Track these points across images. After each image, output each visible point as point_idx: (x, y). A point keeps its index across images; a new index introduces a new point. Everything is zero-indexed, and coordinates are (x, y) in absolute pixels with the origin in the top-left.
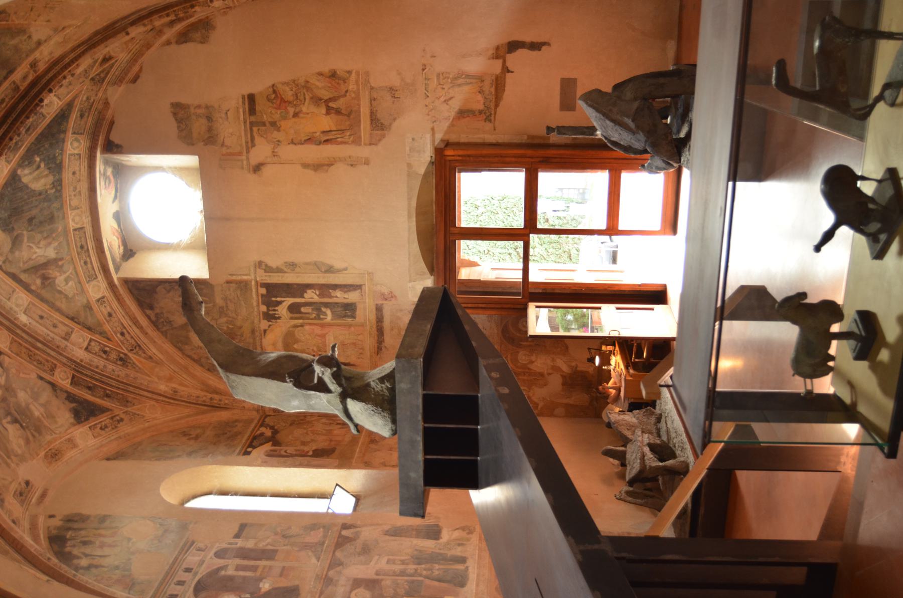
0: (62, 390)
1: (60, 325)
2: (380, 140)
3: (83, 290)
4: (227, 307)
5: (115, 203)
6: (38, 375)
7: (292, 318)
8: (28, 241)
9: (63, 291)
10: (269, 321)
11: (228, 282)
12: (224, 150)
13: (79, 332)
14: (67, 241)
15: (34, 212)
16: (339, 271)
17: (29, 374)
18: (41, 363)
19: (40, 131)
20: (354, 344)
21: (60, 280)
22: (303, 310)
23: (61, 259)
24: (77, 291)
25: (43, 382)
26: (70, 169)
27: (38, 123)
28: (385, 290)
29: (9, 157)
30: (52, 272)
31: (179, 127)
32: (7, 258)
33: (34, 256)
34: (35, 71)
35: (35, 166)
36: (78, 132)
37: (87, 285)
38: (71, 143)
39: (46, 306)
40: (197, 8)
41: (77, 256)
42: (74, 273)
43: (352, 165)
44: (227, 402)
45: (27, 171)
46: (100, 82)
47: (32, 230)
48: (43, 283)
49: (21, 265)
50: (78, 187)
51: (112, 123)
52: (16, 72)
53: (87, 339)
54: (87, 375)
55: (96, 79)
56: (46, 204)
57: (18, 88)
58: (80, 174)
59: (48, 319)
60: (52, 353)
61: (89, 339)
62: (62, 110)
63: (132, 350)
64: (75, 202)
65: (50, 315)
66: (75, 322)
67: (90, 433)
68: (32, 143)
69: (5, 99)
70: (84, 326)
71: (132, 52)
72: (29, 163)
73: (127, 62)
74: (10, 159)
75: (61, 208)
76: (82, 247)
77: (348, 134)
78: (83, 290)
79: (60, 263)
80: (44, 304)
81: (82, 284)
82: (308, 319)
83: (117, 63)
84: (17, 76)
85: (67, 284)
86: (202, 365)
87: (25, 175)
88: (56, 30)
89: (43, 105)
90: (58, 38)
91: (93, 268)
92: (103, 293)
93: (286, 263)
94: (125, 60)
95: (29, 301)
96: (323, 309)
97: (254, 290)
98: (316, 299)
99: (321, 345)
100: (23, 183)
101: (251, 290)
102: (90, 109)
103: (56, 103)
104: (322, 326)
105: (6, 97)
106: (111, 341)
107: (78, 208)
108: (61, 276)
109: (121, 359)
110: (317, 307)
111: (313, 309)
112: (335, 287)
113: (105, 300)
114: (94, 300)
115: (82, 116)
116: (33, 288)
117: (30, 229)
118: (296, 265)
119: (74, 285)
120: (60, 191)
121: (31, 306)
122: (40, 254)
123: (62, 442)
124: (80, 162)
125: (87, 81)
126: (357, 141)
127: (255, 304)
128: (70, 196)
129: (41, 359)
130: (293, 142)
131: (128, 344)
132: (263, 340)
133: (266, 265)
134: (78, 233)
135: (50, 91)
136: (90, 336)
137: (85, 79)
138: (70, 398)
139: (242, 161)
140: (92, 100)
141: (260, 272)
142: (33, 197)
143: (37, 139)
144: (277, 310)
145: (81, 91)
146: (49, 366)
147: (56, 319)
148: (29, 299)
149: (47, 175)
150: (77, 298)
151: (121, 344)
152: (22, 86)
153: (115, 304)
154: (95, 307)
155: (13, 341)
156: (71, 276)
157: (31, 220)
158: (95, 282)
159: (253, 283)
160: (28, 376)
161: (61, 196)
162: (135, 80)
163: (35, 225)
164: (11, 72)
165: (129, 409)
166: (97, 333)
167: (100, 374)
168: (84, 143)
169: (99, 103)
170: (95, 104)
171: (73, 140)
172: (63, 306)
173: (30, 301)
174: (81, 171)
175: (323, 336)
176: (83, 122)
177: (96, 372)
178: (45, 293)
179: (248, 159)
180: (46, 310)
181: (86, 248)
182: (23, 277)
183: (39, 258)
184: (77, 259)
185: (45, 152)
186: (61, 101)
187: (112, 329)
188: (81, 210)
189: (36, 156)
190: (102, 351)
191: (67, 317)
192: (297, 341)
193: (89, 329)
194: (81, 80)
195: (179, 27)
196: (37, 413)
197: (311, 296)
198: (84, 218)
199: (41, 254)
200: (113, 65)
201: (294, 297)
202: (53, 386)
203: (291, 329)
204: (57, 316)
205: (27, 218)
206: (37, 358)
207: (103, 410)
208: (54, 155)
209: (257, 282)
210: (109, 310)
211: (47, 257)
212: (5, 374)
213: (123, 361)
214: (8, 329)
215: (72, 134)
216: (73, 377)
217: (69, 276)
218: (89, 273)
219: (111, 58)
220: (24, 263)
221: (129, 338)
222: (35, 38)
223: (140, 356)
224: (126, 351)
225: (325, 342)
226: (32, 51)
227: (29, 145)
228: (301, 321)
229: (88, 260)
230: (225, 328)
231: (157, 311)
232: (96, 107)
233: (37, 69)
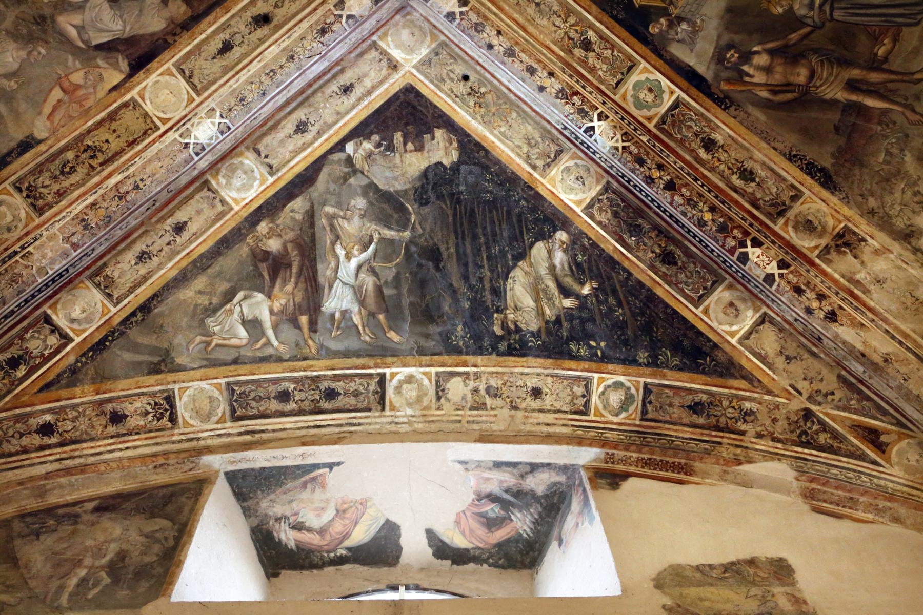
1: (143, 271)
3: (214, 364)
5: (425, 541)
6: (40, 142)
8: (382, 240)
9: (228, 306)
13: (103, 315)
17: (50, 116)
18: (62, 173)
19: (659, 292)
23: (313, 326)
24: (217, 345)
25: (13, 144)
26: (549, 380)
27: (680, 286)
29: (600, 209)
32: (355, 171)
33: (340, 252)
35: (569, 281)
36: (650, 402)
37: (223, 381)
38: (618, 385)
39: (202, 249)
41: (309, 373)
42: (269, 351)
45: (559, 257)
46: (800, 436)
47: (408, 255)
48: (267, 253)
49: (329, 209)
50: (498, 402)
51: (681, 482)
52: (825, 194)
53: (72, 330)
55: (809, 425)
56: (467, 305)
57: (781, 214)
58: (533, 410)
59: (169, 244)
61: (71, 334)
62: (716, 346)
64: (457, 388)
65: (179, 253)
66: (133, 314)
68: (630, 274)
69: (753, 180)
70: (113, 332)
71: (915, 492)
73: (877, 485)
74: (595, 211)
76: (331, 394)
78: (214, 366)
79: (304, 320)
80: (211, 243)
81: (232, 367)
83: (871, 466)
85: (244, 323)
87: (550, 252)
89: (746, 247)
91: (263, 416)
92: (187, 425)
94: (882, 483)
95: (233, 205)
100: (532, 245)
102: (718, 428)
103: (735, 328)
105: (759, 184)
106: (40, 390)
107: (439, 398)
108: (272, 312)
113: (165, 421)
114: (176, 387)
115: (696, 408)
116: (263, 227)
117: (413, 249)
119: (234, 342)
120: (494, 349)
121: (220, 208)
122: (341, 267)
124: (566, 412)
125: (799, 403)
128: (477, 376)
129: (74, 178)
131: (11, 432)
134: (372, 388)
136: (78, 340)
137: (805, 395)
140: (743, 427)
142: (492, 271)
143: (641, 284)
145: (769, 392)
146: (45, 191)
147: (160, 266)
148: (237, 208)
149: (543, 314)
150: (199, 339)
151: (18, 411)
152: (786, 223)
154: (154, 384)
156: (263, 340)
158: (223, 407)
160: (47, 109)
161: (480, 351)
162: (818, 510)
163: (420, 266)
164: (827, 181)
166: (77, 361)
168: (620, 424)
169: (737, 446)
170: (733, 436)
171: (629, 389)
172: (187, 294)
173: (232, 209)
174: (541, 415)
176: (676, 413)
178: (243, 250)
180: (192, 247)
181: (325, 405)
182: (298, 205)
183: (333, 264)
184: (302, 374)
185: (604, 308)
186: (740, 342)
187: (74, 407)
188: (434, 406)
189: (595, 285)
190: (20, 357)
191: (155, 296)
193: (99, 347)
194: (803, 386)
198: (409, 412)
200: (862, 457)
204: (168, 270)
205: (443, 248)
206: (81, 171)
208: (592, 337)
210: (133, 422)
211: (331, 287)
212: (81, 45)
215: (646, 385)
217: (263, 333)
218: (254, 399)
219: (881, 448)
220: (332, 218)
221: (25, 441)
226: (885, 224)
227: (626, 264)
229: (292, 406)
231: (86, 517)
232: (725, 441)
233: (833, 255)
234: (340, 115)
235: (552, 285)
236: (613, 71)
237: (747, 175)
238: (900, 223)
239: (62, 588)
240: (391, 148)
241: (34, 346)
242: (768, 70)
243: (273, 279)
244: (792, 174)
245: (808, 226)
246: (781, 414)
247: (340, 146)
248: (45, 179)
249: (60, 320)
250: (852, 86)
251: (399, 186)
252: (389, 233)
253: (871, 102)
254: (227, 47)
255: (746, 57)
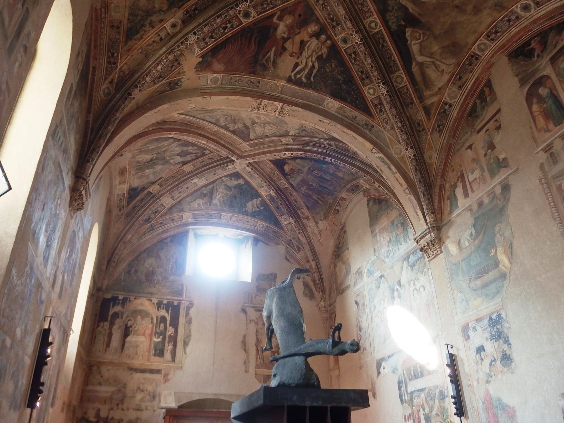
0: (149, 186)
1: (180, 195)
2: (258, 380)
4: (168, 282)
7: (157, 317)
10: (157, 304)
11: (182, 285)
12: (254, 295)
14: (217, 210)
15: (238, 200)
16: (184, 349)
20: (136, 353)
21: (201, 202)
22: (162, 325)
23: (210, 205)
28: (169, 377)
30: (206, 199)
31: (265, 275)
33: (217, 193)
34: (303, 218)
35: (259, 206)
40: (321, 293)
43: (245, 362)
44: (111, 270)
45: (258, 202)
51: (267, 245)
54: (149, 200)
60: (169, 188)
63: (152, 226)
67: (122, 193)
72: (262, 204)
75: (235, 212)
77: (261, 362)
79: (208, 204)
82: (156, 327)
84: (305, 210)
86: (133, 261)
88: (320, 232)
90: (316, 231)
93: (192, 318)
96: (161, 337)
97: (177, 298)
98: (168, 333)
99: (138, 332)
101: (177, 297)
104: (151, 335)
109: (149, 219)
110: (163, 334)
111: (162, 330)
112: (175, 346)
115: (274, 232)
116: (204, 189)
118: (190, 324)
120: (242, 214)
123: (126, 178)
125: (290, 238)
126: (257, 367)
127: (168, 297)
130: (257, 331)
132: (145, 299)
133: (191, 307)
135: (295, 222)
138: (143, 189)
139: (248, 303)
141: (187, 304)
144: (163, 309)
153: (177, 224)
154: (180, 214)
155: (184, 172)
157: (235, 197)
158: (191, 217)
159: (181, 299)
161: (240, 213)
162: (286, 259)
164: (308, 209)
165: (123, 216)
167: (148, 207)
172: (188, 199)
175: (144, 335)
177: (150, 205)
178: (199, 193)
179: (249, 307)
182: (211, 186)
191: (181, 200)
192: (143, 318)
193: (171, 208)
194: (292, 236)
195: (311, 284)
196: (147, 171)
197: (170, 331)
199: (217, 197)
200: (296, 251)
201: (171, 320)
202: (153, 183)
203: (150, 316)
206: (170, 180)
207: (129, 203)
209: (181, 300)
210: (175, 220)
213: (148, 220)
214: (191, 172)
216: (152, 193)
219: (299, 251)
222: (320, 222)
223: (147, 229)
224: (152, 223)
225: (140, 335)
226: (314, 219)
228: (155, 322)
230: (155, 278)
234: (223, 173)
235: (256, 206)
236: (278, 179)
237: (296, 202)
238: (316, 220)
239: (169, 268)
240: (231, 179)
241: (159, 209)
242: (305, 190)
243: (204, 197)
244: (303, 205)
245: (303, 213)
246: (287, 239)
247: (221, 178)
248: (164, 182)
249: (164, 204)
250: (318, 198)
251: (231, 185)
252: (227, 192)
253: (320, 202)
254: (202, 162)
255: (302, 187)
